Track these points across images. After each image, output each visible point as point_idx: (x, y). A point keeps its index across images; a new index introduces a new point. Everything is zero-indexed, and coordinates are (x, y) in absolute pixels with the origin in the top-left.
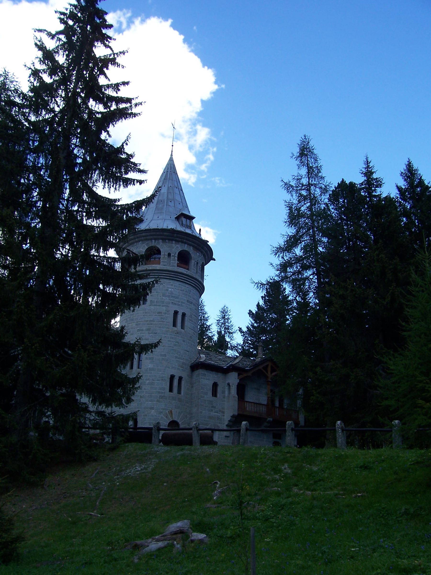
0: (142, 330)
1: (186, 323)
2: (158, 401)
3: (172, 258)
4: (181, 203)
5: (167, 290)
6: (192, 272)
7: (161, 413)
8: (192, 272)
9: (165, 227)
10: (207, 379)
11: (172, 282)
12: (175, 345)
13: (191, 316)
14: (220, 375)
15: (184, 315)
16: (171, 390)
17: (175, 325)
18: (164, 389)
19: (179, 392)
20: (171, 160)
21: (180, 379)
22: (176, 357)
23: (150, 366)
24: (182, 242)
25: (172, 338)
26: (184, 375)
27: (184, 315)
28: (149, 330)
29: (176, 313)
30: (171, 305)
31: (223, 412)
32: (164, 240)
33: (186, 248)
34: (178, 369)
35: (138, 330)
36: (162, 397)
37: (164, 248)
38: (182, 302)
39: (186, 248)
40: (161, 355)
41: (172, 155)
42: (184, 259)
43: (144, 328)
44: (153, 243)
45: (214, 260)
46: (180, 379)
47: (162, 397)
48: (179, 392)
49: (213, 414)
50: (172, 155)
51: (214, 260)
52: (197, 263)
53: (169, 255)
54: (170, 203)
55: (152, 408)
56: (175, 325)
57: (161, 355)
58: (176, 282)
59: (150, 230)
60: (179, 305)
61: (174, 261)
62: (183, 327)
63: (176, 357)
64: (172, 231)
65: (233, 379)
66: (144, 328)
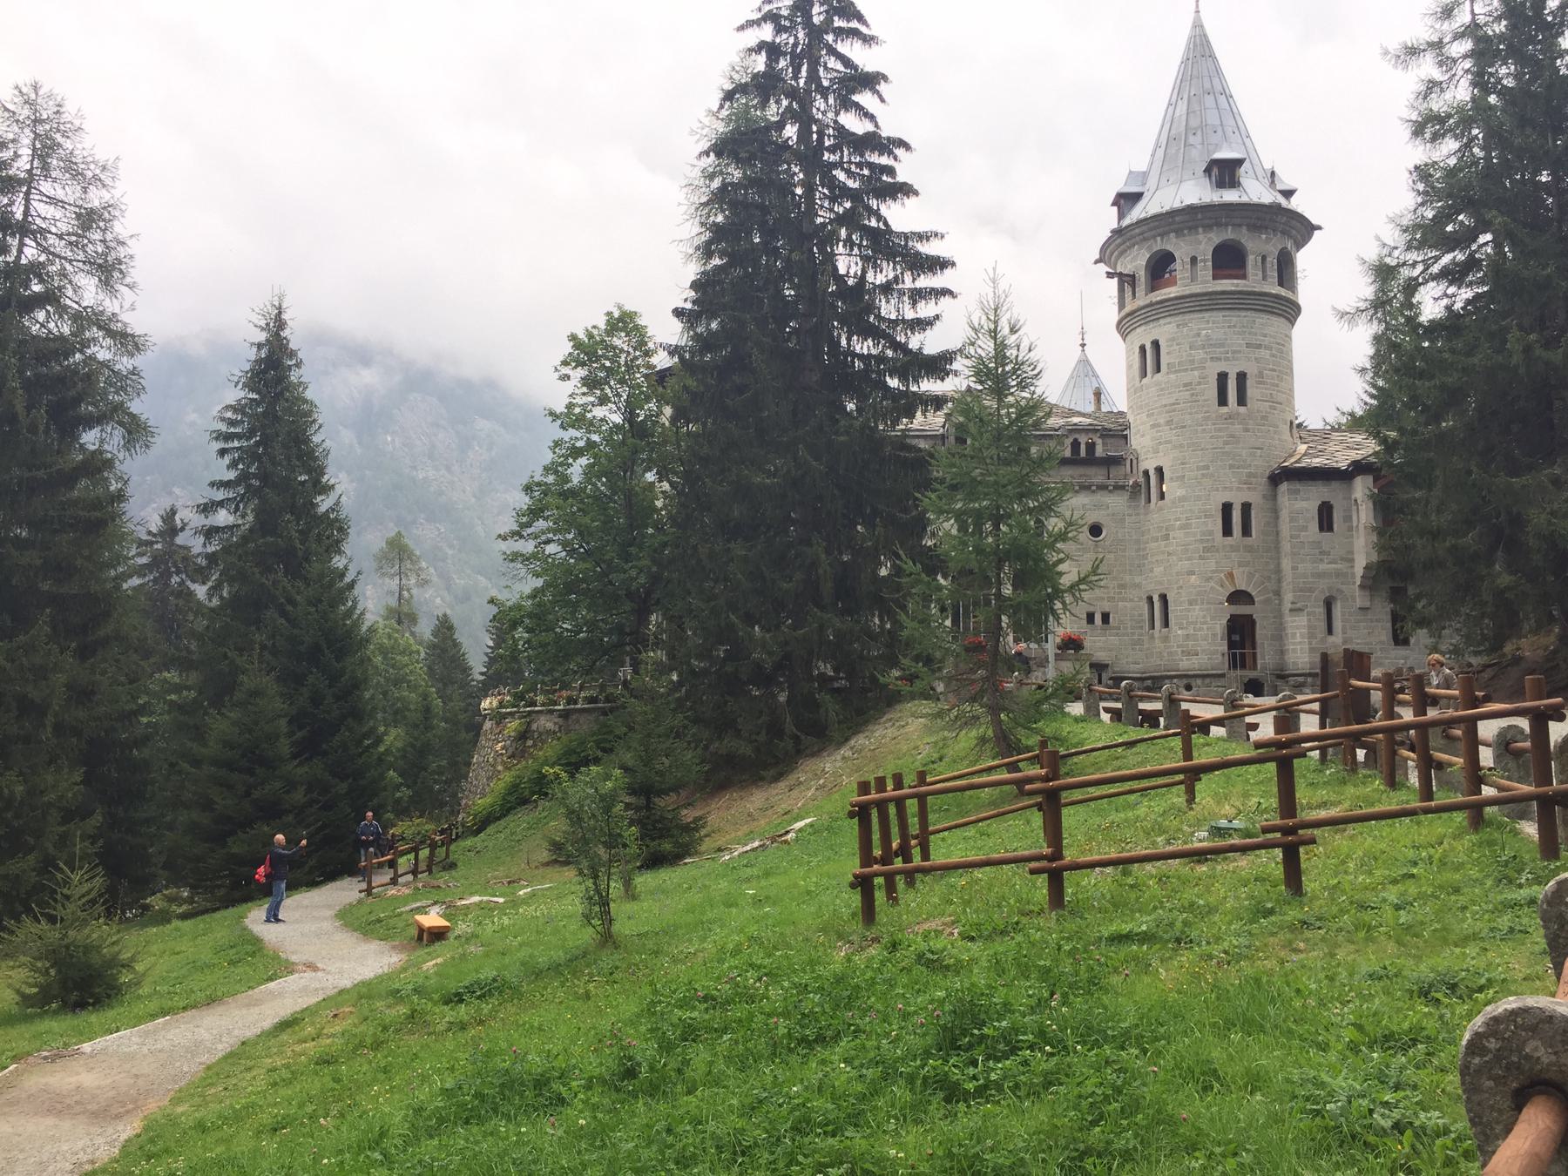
0: (1158, 425)
2: (1201, 558)
3: (1200, 265)
4: (1219, 130)
5: (1199, 335)
7: (1208, 580)
8: (1256, 280)
9: (1177, 205)
10: (1301, 504)
11: (1207, 315)
12: (1226, 443)
13: (1261, 374)
14: (1335, 485)
15: (1242, 377)
16: (1227, 531)
17: (1223, 401)
18: (1211, 533)
19: (1246, 531)
20: (1198, 25)
21: (1246, 508)
22: (1231, 467)
23: (1180, 492)
24: (1219, 225)
25: (1220, 430)
26: (1254, 498)
27: (1242, 377)
28: (1169, 422)
29: (1222, 378)
30: (1209, 364)
31: (1352, 560)
32: (1179, 233)
34: (1239, 489)
37: (1181, 249)
38: (1234, 352)
39: (1229, 234)
40: (1199, 468)
42: (1229, 260)
43: (1162, 421)
44: (1159, 245)
45: (1319, 228)
46: (1246, 508)
48: (1246, 531)
49: (1323, 567)
51: (1319, 228)
52: (1264, 258)
53: (1194, 260)
54: (1192, 139)
55: (1192, 573)
56: (1223, 401)
57: (1199, 468)
58: (1215, 313)
59: (1146, 219)
60: (1227, 359)
61: (1205, 270)
62: (1242, 401)
63: (1231, 467)
64: (1191, 210)
65: (1361, 487)
66: (1162, 421)
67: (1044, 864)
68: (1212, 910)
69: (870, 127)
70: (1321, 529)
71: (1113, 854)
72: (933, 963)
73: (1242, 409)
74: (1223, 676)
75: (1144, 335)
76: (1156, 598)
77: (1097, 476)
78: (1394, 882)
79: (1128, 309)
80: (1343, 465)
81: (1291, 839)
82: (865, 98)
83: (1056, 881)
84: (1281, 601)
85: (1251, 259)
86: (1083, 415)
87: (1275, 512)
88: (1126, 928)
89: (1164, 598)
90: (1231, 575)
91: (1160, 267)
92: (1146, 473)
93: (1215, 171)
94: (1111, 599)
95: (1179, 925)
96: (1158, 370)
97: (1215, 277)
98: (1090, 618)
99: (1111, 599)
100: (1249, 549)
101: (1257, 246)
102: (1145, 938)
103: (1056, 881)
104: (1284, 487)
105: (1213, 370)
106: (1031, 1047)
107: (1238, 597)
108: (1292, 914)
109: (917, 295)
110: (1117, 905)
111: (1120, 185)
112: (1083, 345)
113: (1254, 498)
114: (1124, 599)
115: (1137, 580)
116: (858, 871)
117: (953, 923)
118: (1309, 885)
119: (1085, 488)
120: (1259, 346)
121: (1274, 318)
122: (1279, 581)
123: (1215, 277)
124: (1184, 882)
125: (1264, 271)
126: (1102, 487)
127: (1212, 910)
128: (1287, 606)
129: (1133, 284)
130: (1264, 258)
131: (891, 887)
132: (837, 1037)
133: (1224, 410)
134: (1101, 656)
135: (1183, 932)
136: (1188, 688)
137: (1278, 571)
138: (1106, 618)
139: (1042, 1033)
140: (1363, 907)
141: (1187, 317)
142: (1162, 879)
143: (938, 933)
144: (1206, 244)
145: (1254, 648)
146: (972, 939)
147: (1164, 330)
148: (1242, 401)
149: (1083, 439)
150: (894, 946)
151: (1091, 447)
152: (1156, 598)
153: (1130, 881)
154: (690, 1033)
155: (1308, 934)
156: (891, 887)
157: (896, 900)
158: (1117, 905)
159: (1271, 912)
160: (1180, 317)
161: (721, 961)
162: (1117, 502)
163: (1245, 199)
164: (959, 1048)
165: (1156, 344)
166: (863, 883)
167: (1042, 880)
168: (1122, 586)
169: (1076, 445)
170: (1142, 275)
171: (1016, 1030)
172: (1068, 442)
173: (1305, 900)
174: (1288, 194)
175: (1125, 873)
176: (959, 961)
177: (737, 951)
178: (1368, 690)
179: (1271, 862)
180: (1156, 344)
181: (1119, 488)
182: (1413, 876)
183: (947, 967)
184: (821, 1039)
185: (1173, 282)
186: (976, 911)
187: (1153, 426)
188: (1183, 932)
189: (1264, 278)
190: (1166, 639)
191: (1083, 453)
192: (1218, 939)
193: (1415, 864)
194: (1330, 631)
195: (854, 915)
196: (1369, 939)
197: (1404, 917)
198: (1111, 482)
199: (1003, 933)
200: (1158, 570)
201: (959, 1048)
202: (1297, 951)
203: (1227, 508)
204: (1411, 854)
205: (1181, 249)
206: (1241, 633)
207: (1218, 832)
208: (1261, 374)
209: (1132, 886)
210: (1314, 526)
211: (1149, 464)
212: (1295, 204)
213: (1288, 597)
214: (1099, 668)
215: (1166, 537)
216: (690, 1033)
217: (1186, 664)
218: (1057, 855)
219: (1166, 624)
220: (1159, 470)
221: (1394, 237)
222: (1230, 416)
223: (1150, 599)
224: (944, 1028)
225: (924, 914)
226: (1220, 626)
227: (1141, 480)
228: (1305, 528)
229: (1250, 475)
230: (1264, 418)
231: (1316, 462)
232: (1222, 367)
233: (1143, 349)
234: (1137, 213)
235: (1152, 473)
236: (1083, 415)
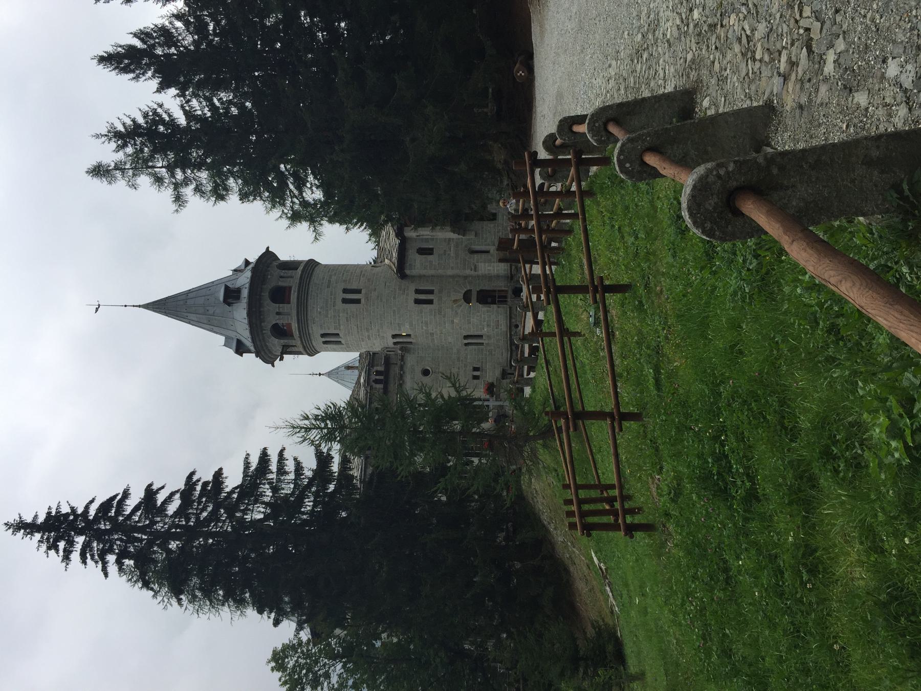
1: (354, 287)
3: (281, 310)
6: (293, 282)
8: (293, 282)
9: (246, 321)
10: (418, 264)
11: (309, 308)
12: (381, 300)
13: (345, 281)
15: (345, 291)
16: (430, 302)
17: (358, 301)
19: (431, 292)
20: (147, 306)
21: (418, 291)
22: (394, 298)
27: (345, 291)
28: (368, 330)
29: (345, 301)
30: (336, 308)
31: (449, 239)
33: (266, 295)
34: (407, 295)
35: (369, 338)
36: (440, 312)
37: (271, 319)
39: (266, 295)
41: (139, 306)
42: (280, 295)
45: (268, 248)
46: (418, 291)
47: (440, 312)
48: (431, 292)
50: (139, 306)
51: (268, 248)
52: (281, 277)
53: (278, 313)
54: (211, 312)
55: (453, 322)
56: (358, 301)
60: (335, 298)
61: (285, 308)
62: (358, 291)
63: (394, 298)
64: (249, 314)
65: (410, 233)
67: (616, 425)
68: (640, 332)
69: (178, 496)
70: (431, 254)
71: (609, 382)
72: (677, 493)
73: (363, 292)
74: (510, 308)
75: (317, 341)
76: (466, 341)
77: (395, 370)
78: (623, 237)
79: (301, 350)
80: (398, 242)
81: (599, 289)
82: (161, 498)
83: (625, 417)
84: (471, 276)
85: (280, 284)
86: (360, 376)
87: (420, 277)
88: (652, 381)
89: (466, 337)
90: (455, 301)
91: (281, 332)
92: (395, 343)
93: (230, 300)
94: (466, 366)
95: (649, 352)
96: (338, 334)
97: (289, 303)
98: (476, 378)
99: (466, 366)
100: (441, 291)
101: (274, 279)
102: (657, 370)
103: (625, 417)
104: (408, 272)
105: (340, 305)
106: (724, 446)
107: (467, 298)
108: (641, 291)
109: (281, 471)
110: (639, 382)
111: (231, 352)
112: (320, 374)
113: (412, 288)
114: (466, 358)
115: (455, 350)
116: (622, 533)
117: (652, 478)
118: (625, 280)
119: (401, 377)
120: (329, 281)
121: (315, 273)
122: (459, 276)
123: (289, 303)
124: (624, 345)
125: (288, 277)
126: (402, 368)
127: (640, 332)
128: (473, 273)
129: (289, 346)
130: (281, 277)
131: (632, 512)
132: (725, 562)
133: (363, 301)
134: (498, 373)
135: (653, 350)
136: (517, 326)
137: (453, 277)
138: (476, 369)
139: (716, 438)
140: (636, 254)
141: (309, 318)
142: (624, 357)
143: (658, 488)
144: (270, 308)
145: (495, 291)
146: (661, 468)
147: (316, 331)
148: (358, 291)
149: (373, 377)
150: (667, 514)
151: (378, 373)
152: (466, 341)
153: (625, 374)
154: (727, 653)
155: (652, 285)
156: (632, 512)
157: (640, 509)
158: (639, 382)
159: (640, 302)
160: (309, 322)
161: (680, 625)
162: (410, 360)
163: (247, 286)
164: (726, 488)
165: (323, 335)
166: (630, 530)
167: (626, 424)
168: (458, 359)
169: (376, 381)
170: (283, 342)
171: (713, 454)
172: (375, 386)
173: (633, 283)
174: (247, 263)
175: (621, 376)
176: (675, 478)
177: (674, 613)
178: (519, 240)
179: (612, 299)
180: (323, 335)
181: (402, 358)
182: (619, 228)
183: (678, 485)
184: (726, 570)
185: (289, 325)
186: (645, 463)
187: (369, 338)
188: (653, 350)
189: (292, 277)
190: (489, 337)
191: (382, 377)
192: (656, 331)
193: (613, 226)
194: (488, 252)
195: (650, 536)
196: (654, 253)
197: (642, 235)
198: (399, 363)
199: (657, 449)
200: (450, 339)
201: (726, 488)
202: (661, 291)
203: (417, 302)
204: (608, 227)
205: (271, 319)
206: (487, 298)
207: (597, 323)
208: (345, 281)
209: (628, 374)
210: (430, 257)
211: (390, 342)
212: (253, 259)
213: (468, 272)
214: (504, 374)
215: (432, 334)
216: (727, 653)
217: (504, 327)
218: (611, 415)
219: (480, 336)
220: (394, 336)
221: (277, 212)
222: (367, 298)
223: (466, 344)
224: (714, 495)
225: (650, 492)
226: (483, 309)
227: (399, 346)
228: (431, 262)
229: (400, 289)
230: (369, 280)
231: (395, 255)
232: (339, 301)
233: (325, 343)
234: (248, 343)
235: (395, 340)
236: (360, 376)
